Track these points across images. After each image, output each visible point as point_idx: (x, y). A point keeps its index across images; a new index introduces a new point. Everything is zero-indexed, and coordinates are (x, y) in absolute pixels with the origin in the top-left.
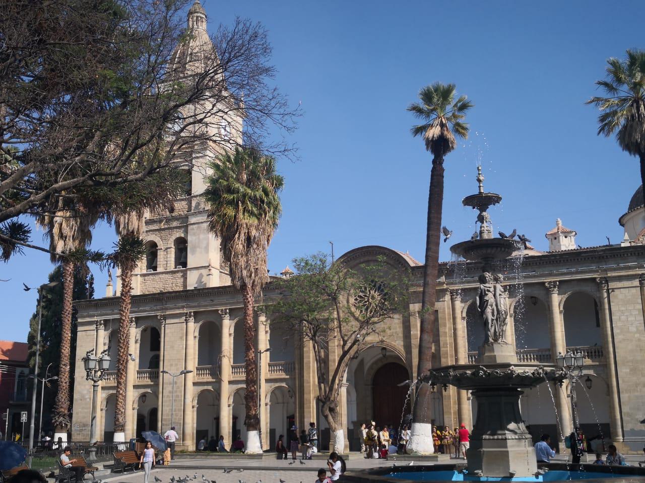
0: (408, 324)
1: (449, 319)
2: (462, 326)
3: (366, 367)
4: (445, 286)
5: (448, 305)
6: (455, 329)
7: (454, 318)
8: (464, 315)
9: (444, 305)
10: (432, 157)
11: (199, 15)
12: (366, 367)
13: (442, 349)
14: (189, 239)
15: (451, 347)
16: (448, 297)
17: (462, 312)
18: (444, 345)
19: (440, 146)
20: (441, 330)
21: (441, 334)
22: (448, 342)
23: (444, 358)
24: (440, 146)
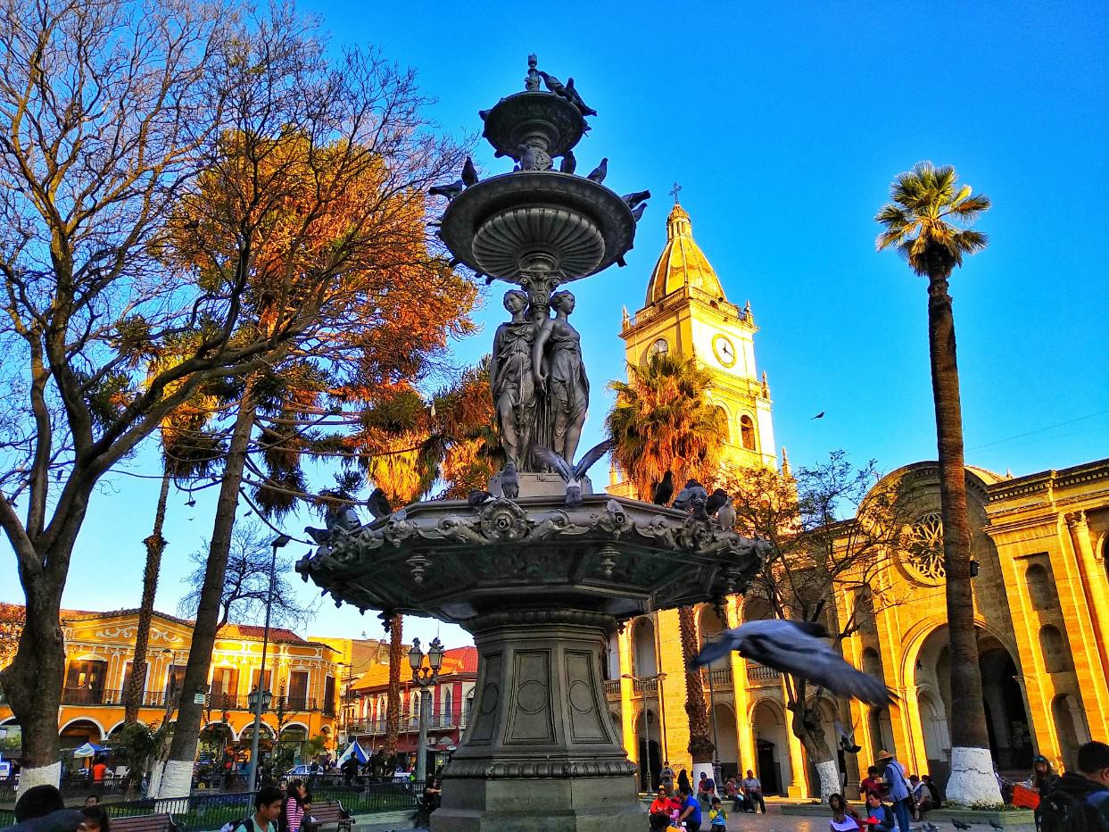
0: (999, 581)
1: (1071, 565)
4: (1055, 510)
5: (1065, 541)
8: (1099, 555)
9: (1058, 543)
10: (925, 281)
11: (679, 219)
13: (1066, 618)
15: (1083, 613)
16: (1061, 527)
17: (1095, 554)
18: (1068, 610)
19: (936, 259)
20: (1059, 585)
21: (1059, 592)
22: (1076, 604)
23: (1074, 632)
24: (936, 259)
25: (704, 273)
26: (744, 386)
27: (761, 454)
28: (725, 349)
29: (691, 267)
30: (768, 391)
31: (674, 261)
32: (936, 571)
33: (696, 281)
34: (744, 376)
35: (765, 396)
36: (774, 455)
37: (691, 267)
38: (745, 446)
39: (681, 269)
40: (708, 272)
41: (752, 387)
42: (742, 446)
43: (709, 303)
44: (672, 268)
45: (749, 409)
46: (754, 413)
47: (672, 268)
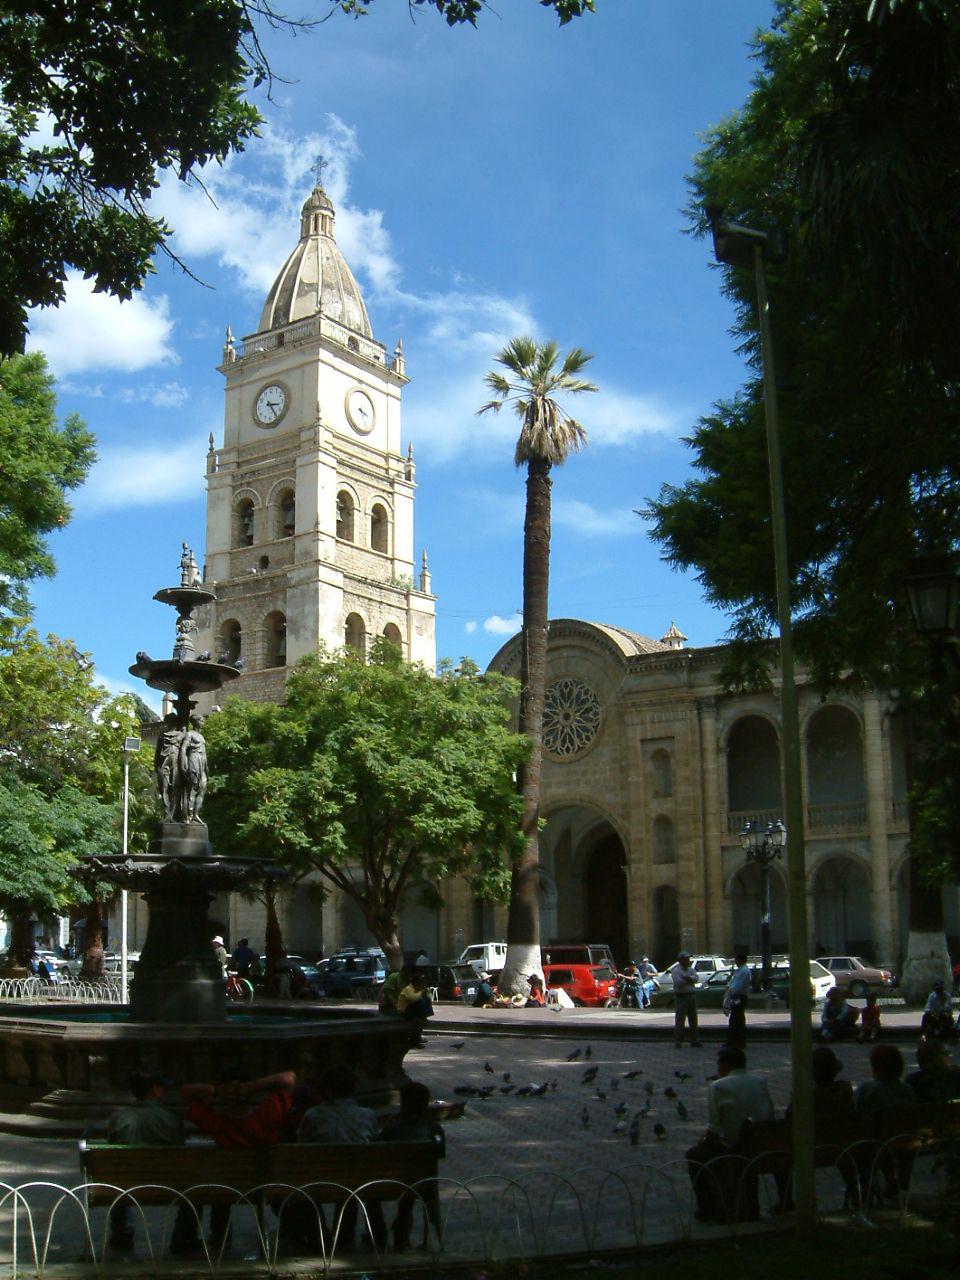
2: (716, 766)
3: (576, 840)
6: (704, 772)
7: (702, 751)
8: (722, 743)
12: (576, 840)
14: (288, 613)
25: (345, 296)
26: (381, 462)
27: (392, 560)
28: (360, 410)
29: (327, 285)
30: (413, 471)
31: (305, 274)
32: (581, 739)
33: (332, 308)
34: (382, 448)
35: (408, 478)
36: (411, 560)
37: (327, 285)
38: (374, 546)
39: (313, 287)
40: (350, 293)
41: (393, 463)
42: (369, 547)
43: (346, 342)
44: (301, 281)
45: (385, 495)
46: (390, 500)
47: (301, 281)
